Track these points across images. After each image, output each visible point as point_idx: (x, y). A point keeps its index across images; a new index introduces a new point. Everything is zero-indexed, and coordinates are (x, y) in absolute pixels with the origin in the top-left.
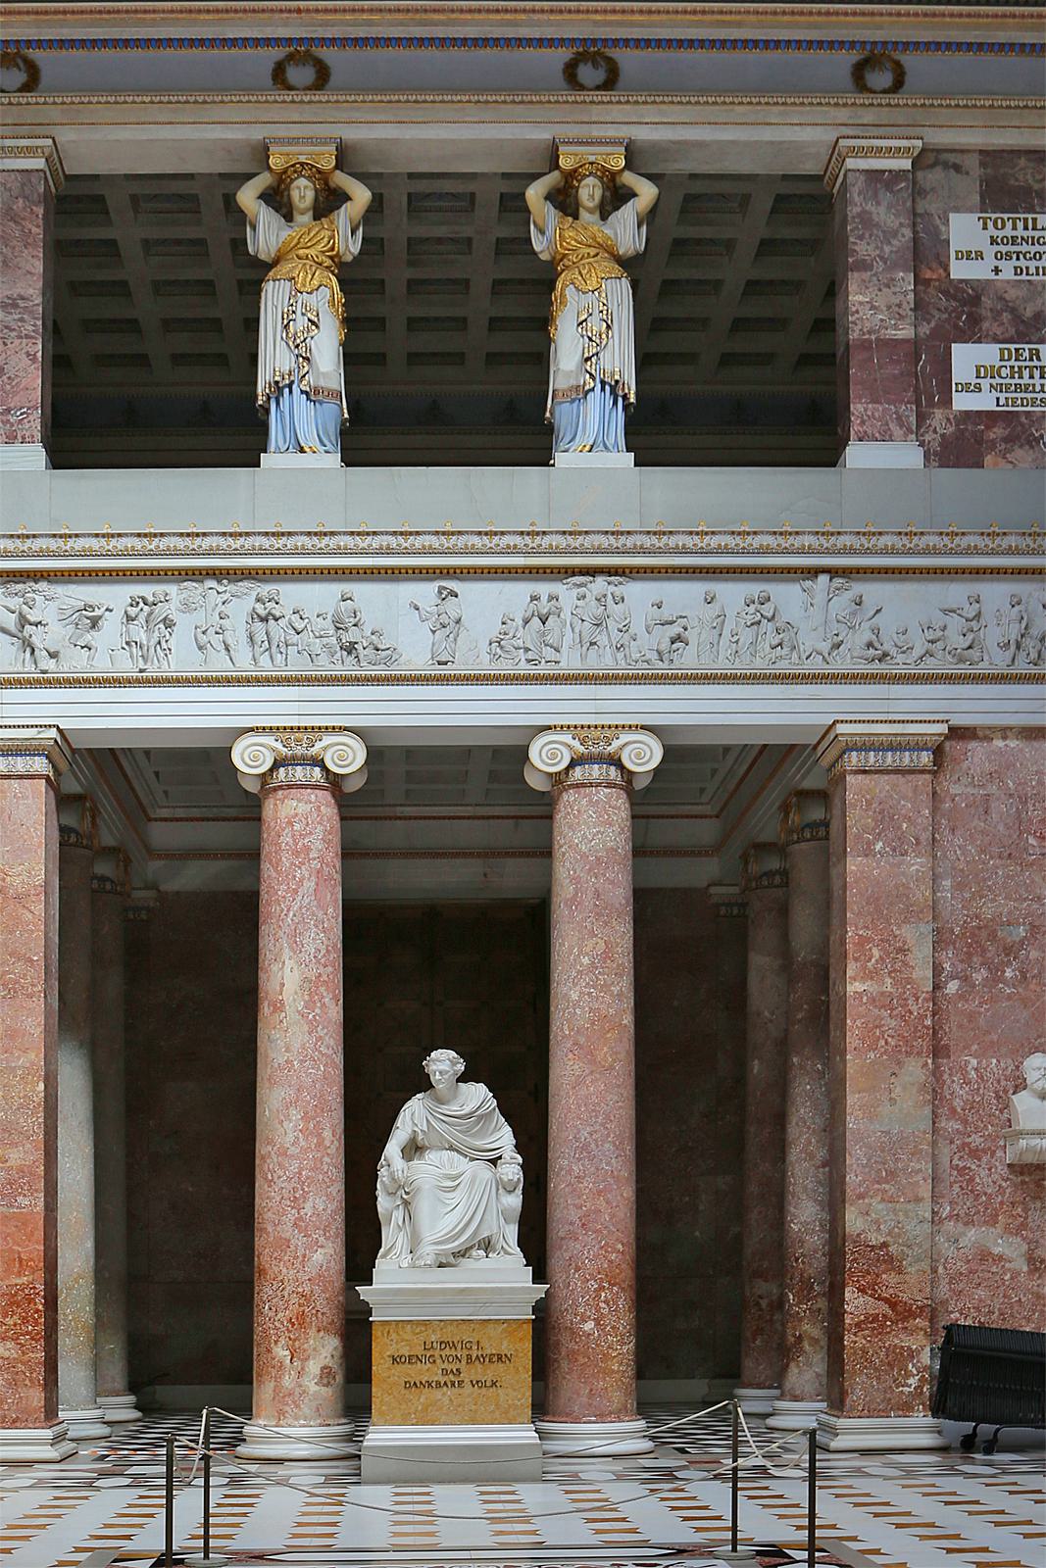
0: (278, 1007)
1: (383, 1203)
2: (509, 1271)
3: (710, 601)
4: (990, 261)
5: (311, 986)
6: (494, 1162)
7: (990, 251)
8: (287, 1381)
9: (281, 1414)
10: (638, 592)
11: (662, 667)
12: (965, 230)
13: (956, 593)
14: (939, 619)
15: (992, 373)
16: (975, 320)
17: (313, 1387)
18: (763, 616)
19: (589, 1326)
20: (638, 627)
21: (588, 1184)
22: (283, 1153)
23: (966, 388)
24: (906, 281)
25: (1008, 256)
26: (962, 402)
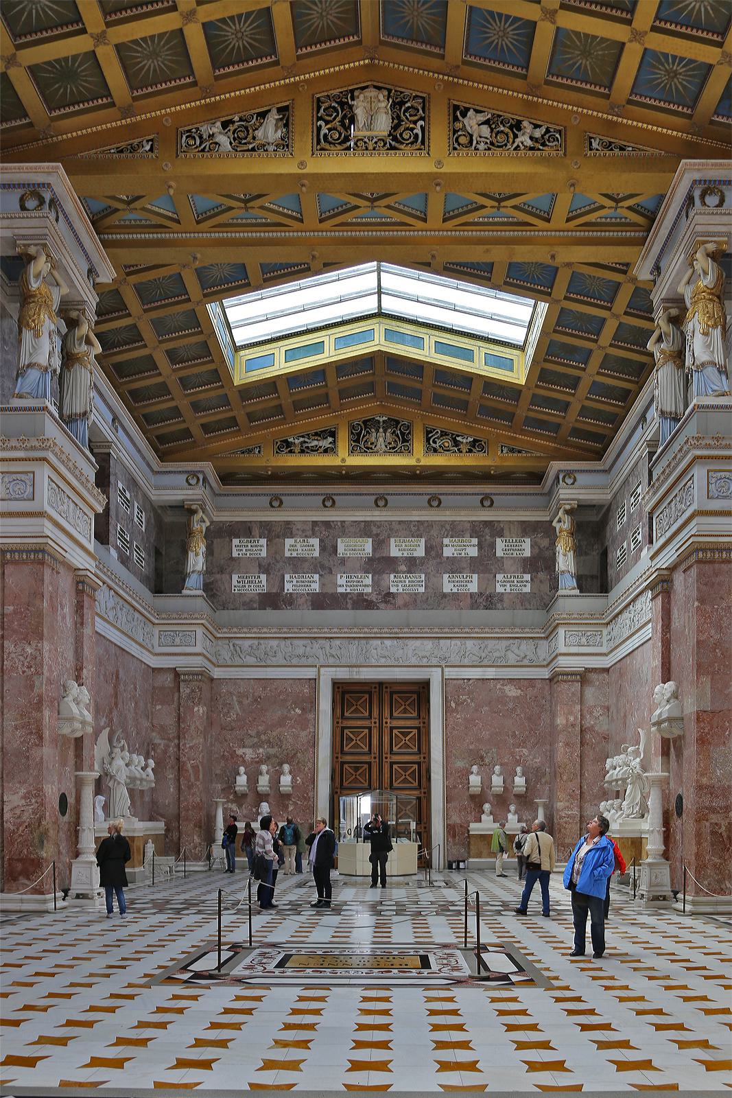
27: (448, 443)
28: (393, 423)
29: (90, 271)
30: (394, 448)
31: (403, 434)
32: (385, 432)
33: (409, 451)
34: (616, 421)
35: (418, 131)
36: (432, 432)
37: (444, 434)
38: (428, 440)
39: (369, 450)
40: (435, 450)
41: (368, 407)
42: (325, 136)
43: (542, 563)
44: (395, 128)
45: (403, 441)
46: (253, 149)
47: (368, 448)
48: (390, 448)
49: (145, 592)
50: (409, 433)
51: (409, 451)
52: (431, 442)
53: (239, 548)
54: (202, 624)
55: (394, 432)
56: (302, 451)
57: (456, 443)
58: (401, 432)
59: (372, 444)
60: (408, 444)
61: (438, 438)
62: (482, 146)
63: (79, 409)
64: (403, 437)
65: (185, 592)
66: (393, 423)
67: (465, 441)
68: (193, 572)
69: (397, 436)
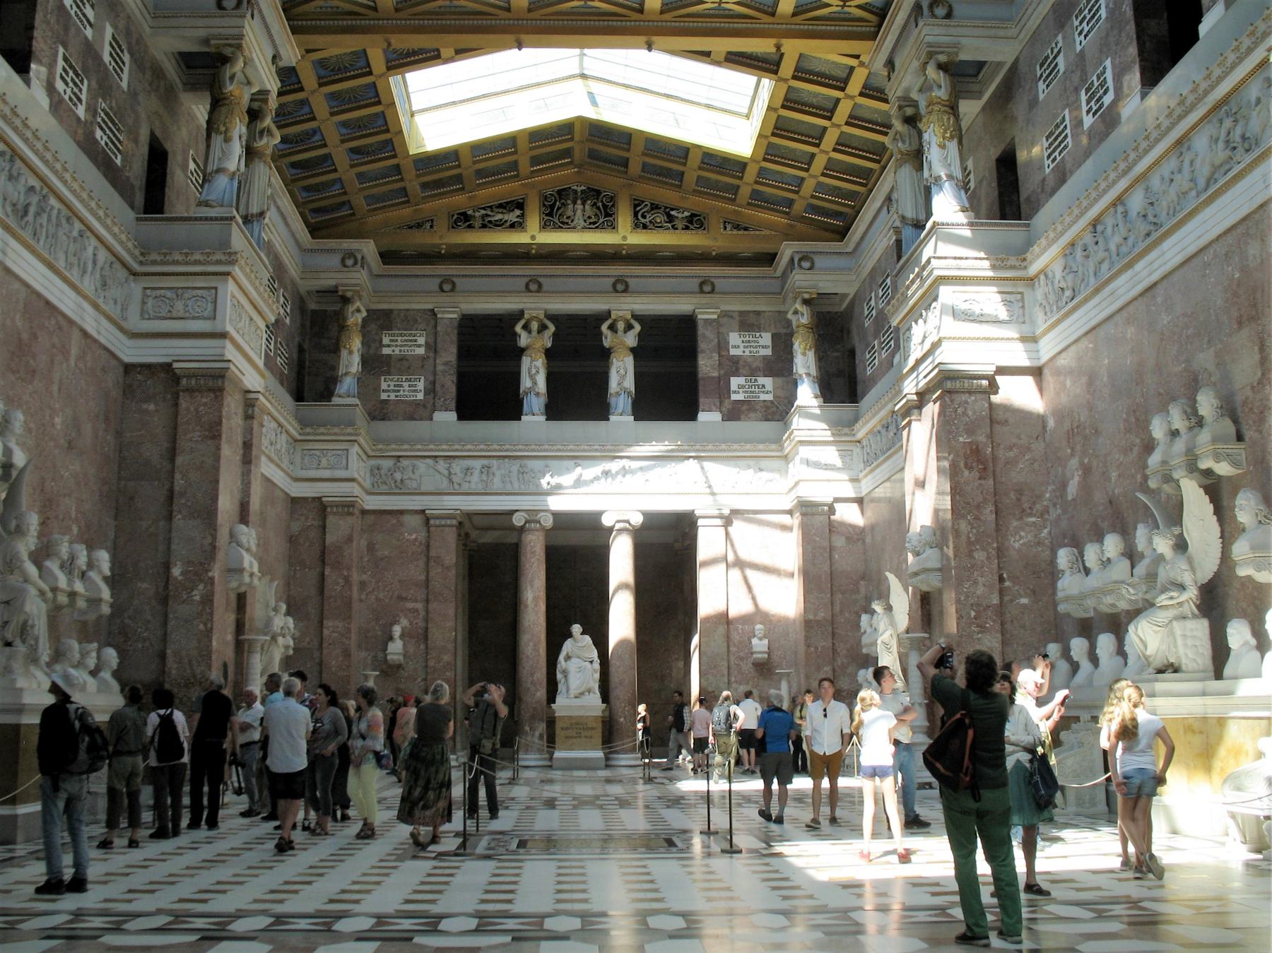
0: (526, 606)
1: (559, 676)
2: (595, 700)
4: (742, 349)
6: (591, 662)
7: (742, 345)
9: (527, 750)
12: (734, 338)
15: (743, 387)
16: (737, 369)
17: (536, 740)
19: (622, 720)
21: (621, 669)
22: (528, 657)
23: (735, 392)
24: (716, 357)
25: (747, 347)
26: (734, 397)
27: (660, 218)
28: (593, 193)
29: (274, 57)
30: (595, 223)
31: (604, 205)
32: (584, 204)
33: (613, 227)
34: (859, 201)
36: (639, 205)
37: (655, 207)
38: (636, 214)
39: (565, 225)
40: (645, 227)
43: (780, 365)
45: (605, 216)
47: (563, 223)
48: (590, 223)
50: (613, 206)
52: (639, 217)
53: (392, 345)
55: (595, 204)
57: (671, 219)
58: (603, 205)
59: (568, 218)
60: (611, 219)
61: (647, 212)
63: (254, 209)
64: (605, 211)
65: (336, 400)
66: (593, 193)
67: (680, 215)
69: (598, 208)
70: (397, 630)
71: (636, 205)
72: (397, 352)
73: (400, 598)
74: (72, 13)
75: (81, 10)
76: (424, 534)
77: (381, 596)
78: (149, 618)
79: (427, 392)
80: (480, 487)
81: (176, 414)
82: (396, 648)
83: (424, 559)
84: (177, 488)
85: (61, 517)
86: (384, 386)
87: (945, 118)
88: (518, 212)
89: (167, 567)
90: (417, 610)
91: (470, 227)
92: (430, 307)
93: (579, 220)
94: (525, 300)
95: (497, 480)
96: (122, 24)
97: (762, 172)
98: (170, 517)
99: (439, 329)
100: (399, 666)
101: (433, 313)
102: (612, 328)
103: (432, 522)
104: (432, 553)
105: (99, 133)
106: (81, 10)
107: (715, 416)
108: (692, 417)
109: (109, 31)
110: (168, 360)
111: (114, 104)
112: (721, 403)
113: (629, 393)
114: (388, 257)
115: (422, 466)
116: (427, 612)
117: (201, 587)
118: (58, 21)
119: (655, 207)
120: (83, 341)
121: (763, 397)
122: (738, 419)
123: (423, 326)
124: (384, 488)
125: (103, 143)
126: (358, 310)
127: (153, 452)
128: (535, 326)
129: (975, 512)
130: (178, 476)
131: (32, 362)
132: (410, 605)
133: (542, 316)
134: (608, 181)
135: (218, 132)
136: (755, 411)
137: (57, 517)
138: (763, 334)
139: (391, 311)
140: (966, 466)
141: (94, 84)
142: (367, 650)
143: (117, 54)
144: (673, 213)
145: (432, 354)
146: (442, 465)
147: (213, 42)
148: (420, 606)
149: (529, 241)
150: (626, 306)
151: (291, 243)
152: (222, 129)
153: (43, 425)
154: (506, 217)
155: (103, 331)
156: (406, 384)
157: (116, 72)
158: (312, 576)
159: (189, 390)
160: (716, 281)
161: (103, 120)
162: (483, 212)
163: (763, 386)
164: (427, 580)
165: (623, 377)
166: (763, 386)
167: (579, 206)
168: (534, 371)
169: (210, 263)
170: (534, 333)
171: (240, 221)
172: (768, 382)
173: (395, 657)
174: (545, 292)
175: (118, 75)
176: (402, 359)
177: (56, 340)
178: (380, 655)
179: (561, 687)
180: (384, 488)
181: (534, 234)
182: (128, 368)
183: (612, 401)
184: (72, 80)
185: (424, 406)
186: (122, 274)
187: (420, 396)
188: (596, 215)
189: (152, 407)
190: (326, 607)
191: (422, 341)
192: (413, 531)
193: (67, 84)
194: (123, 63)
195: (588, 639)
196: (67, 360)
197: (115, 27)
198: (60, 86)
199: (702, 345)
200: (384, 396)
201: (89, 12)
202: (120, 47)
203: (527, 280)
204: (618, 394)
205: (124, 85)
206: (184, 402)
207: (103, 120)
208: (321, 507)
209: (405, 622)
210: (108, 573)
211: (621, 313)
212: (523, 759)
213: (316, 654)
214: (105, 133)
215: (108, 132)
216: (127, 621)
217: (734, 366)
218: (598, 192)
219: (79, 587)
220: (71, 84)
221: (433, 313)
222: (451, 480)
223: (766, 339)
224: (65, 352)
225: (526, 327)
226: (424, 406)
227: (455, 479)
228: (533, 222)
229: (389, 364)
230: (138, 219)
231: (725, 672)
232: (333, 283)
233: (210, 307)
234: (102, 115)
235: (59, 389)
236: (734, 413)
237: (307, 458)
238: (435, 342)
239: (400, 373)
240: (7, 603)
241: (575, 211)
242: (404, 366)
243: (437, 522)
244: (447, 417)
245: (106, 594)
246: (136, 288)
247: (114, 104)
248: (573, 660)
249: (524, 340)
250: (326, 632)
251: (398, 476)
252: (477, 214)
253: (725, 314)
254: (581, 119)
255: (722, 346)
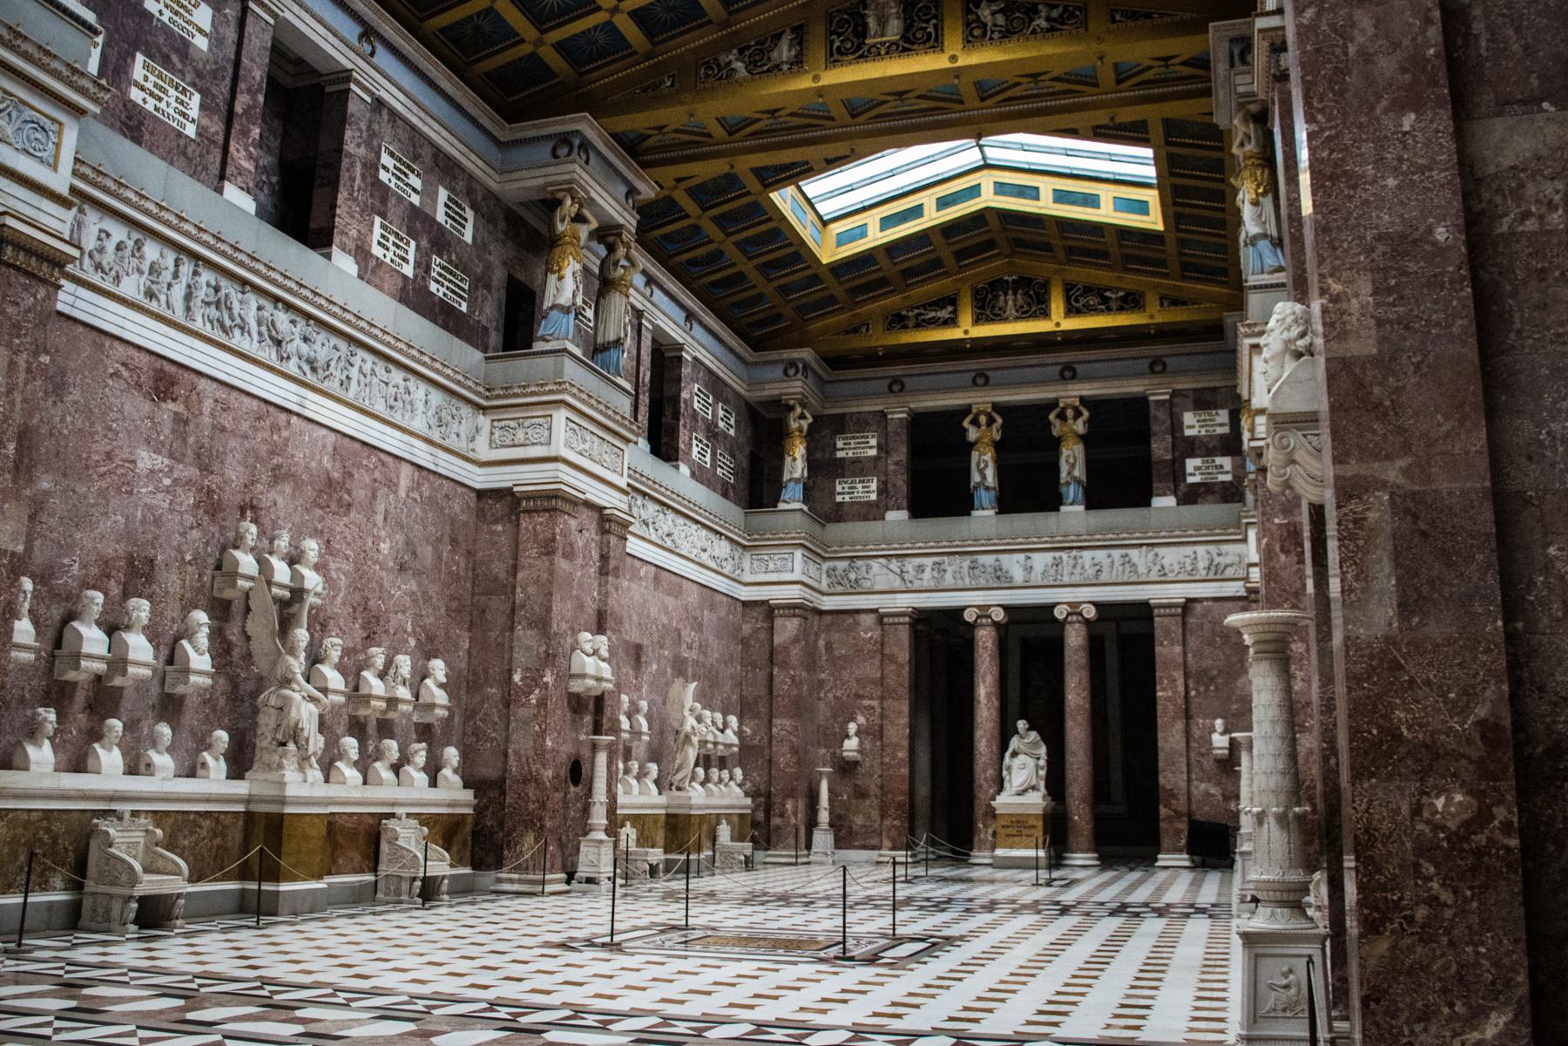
0: (979, 702)
3: (1110, 556)
4: (1197, 429)
5: (988, 695)
7: (1197, 425)
8: (982, 836)
10: (1087, 554)
11: (1095, 581)
13: (1188, 550)
14: (1183, 560)
16: (1193, 450)
18: (1125, 560)
20: (1087, 567)
23: (1191, 474)
24: (1169, 438)
26: (1190, 480)
28: (1024, 283)
30: (1027, 312)
31: (1037, 294)
33: (1045, 314)
35: (931, 30)
38: (1068, 300)
39: (998, 317)
41: (984, 270)
42: (838, 48)
44: (907, 28)
46: (768, 71)
47: (995, 315)
49: (731, 511)
51: (1045, 314)
53: (845, 448)
54: (802, 545)
56: (918, 326)
57: (1105, 300)
59: (1000, 309)
62: (996, 36)
65: (782, 506)
66: (1024, 283)
67: (1113, 296)
68: (790, 480)
69: (1030, 297)
70: (852, 727)
71: (1068, 289)
72: (850, 455)
73: (858, 696)
74: (392, 185)
75: (402, 181)
76: (878, 632)
77: (839, 694)
78: (497, 719)
79: (880, 492)
80: (932, 585)
81: (518, 534)
82: (851, 744)
83: (879, 656)
84: (517, 601)
85: (392, 631)
86: (839, 488)
87: (1259, 173)
88: (950, 308)
89: (510, 672)
90: (873, 708)
91: (905, 327)
92: (880, 408)
93: (1011, 310)
94: (973, 394)
95: (949, 577)
96: (460, 185)
97: (1182, 243)
98: (512, 629)
99: (889, 429)
100: (856, 763)
101: (883, 414)
102: (1062, 416)
103: (886, 620)
104: (887, 651)
105: (433, 287)
106: (402, 181)
107: (1169, 501)
108: (1148, 504)
109: (443, 194)
110: (509, 484)
111: (454, 257)
112: (1176, 486)
113: (1079, 482)
114: (835, 361)
115: (875, 564)
116: (882, 709)
117: (537, 691)
118: (372, 196)
119: (1088, 290)
120: (417, 474)
121: (1222, 478)
122: (1195, 502)
123: (874, 428)
124: (839, 589)
125: (441, 294)
126: (802, 417)
127: (499, 569)
128: (983, 419)
129: (1294, 601)
130: (518, 590)
131: (346, 496)
132: (866, 702)
133: (989, 410)
134: (1039, 268)
135: (553, 272)
136: (1213, 493)
137: (386, 632)
138: (1220, 412)
139: (844, 415)
140: (1282, 551)
141: (424, 243)
142: (826, 747)
143: (457, 213)
144: (1108, 294)
145: (883, 455)
146: (894, 564)
147: (549, 189)
148: (875, 703)
149: (962, 336)
150: (1075, 393)
151: (730, 358)
152: (556, 268)
153: (365, 551)
154: (940, 314)
155: (441, 463)
156: (859, 486)
157: (456, 229)
158: (761, 675)
159: (528, 511)
160: (1167, 360)
161: (440, 275)
162: (916, 311)
163: (1222, 467)
164: (882, 678)
165: (1073, 466)
166: (1222, 467)
167: (1010, 297)
168: (982, 465)
169: (544, 393)
170: (984, 428)
171: (578, 352)
172: (1226, 462)
173: (851, 754)
174: (993, 385)
175: (458, 231)
176: (856, 461)
177: (377, 475)
178: (838, 751)
179: (1006, 785)
180: (839, 589)
181: (968, 328)
182: (481, 494)
183: (1063, 490)
184: (394, 244)
185: (878, 507)
186: (466, 410)
187: (874, 497)
188: (1029, 304)
189: (500, 528)
190: (775, 706)
191: (873, 442)
192: (868, 631)
193: (388, 249)
194: (466, 220)
195: (1034, 735)
196: (395, 492)
197: (452, 189)
198: (377, 251)
199: (1155, 428)
200: (839, 499)
201: (416, 182)
202: (459, 206)
203: (973, 374)
204: (1068, 484)
205: (468, 237)
206: (525, 522)
207: (440, 275)
208: (769, 611)
209: (861, 720)
210: (444, 680)
211: (1069, 401)
212: (977, 857)
213: (767, 752)
214: (443, 285)
215: (446, 283)
216: (479, 723)
217: (1192, 447)
218: (1031, 280)
219: (403, 693)
220: (392, 248)
221: (883, 414)
222: (903, 579)
223: (1223, 416)
224: (392, 485)
225: (975, 422)
226: (878, 507)
227: (906, 576)
228: (966, 318)
229: (843, 468)
230: (486, 358)
231: (1185, 769)
232: (777, 392)
233: (546, 433)
234: (438, 269)
235: (385, 519)
236: (1190, 496)
237: (755, 563)
238: (886, 443)
239: (854, 475)
240: (281, 709)
241: (1006, 302)
242: (858, 468)
243: (891, 620)
244: (897, 516)
245: (441, 697)
246: (484, 421)
247: (454, 257)
248: (1022, 757)
249: (973, 434)
250: (775, 730)
251: (852, 576)
252: (910, 314)
253: (1175, 394)
254: (987, 209)
255: (1176, 426)
